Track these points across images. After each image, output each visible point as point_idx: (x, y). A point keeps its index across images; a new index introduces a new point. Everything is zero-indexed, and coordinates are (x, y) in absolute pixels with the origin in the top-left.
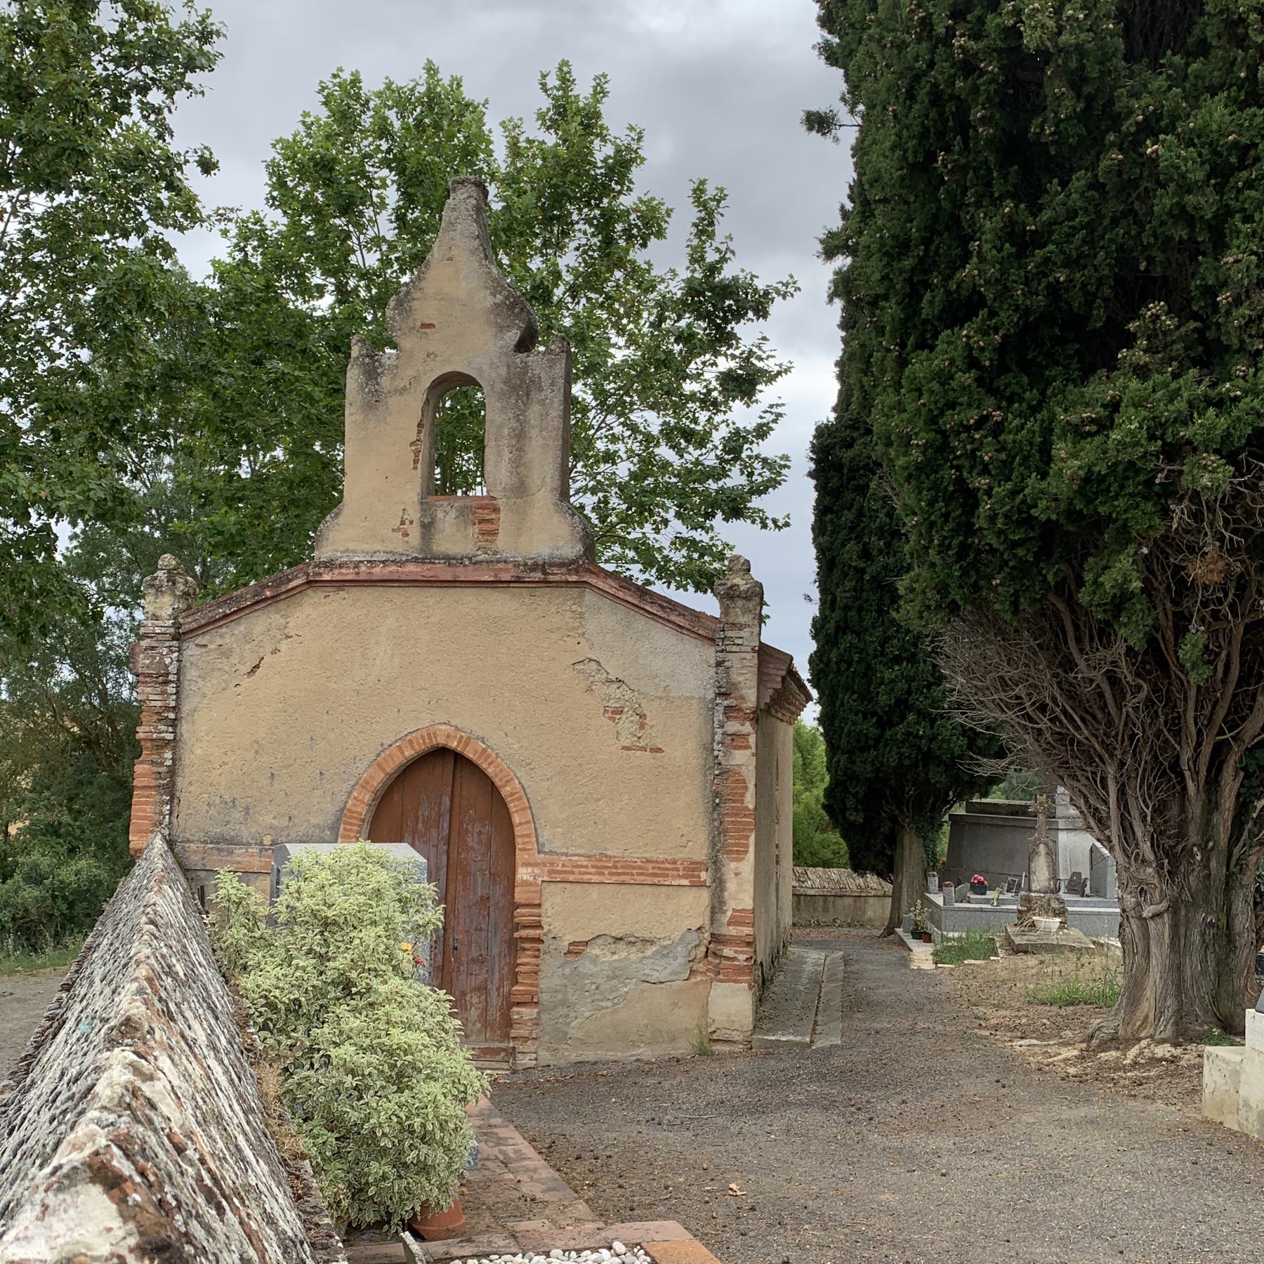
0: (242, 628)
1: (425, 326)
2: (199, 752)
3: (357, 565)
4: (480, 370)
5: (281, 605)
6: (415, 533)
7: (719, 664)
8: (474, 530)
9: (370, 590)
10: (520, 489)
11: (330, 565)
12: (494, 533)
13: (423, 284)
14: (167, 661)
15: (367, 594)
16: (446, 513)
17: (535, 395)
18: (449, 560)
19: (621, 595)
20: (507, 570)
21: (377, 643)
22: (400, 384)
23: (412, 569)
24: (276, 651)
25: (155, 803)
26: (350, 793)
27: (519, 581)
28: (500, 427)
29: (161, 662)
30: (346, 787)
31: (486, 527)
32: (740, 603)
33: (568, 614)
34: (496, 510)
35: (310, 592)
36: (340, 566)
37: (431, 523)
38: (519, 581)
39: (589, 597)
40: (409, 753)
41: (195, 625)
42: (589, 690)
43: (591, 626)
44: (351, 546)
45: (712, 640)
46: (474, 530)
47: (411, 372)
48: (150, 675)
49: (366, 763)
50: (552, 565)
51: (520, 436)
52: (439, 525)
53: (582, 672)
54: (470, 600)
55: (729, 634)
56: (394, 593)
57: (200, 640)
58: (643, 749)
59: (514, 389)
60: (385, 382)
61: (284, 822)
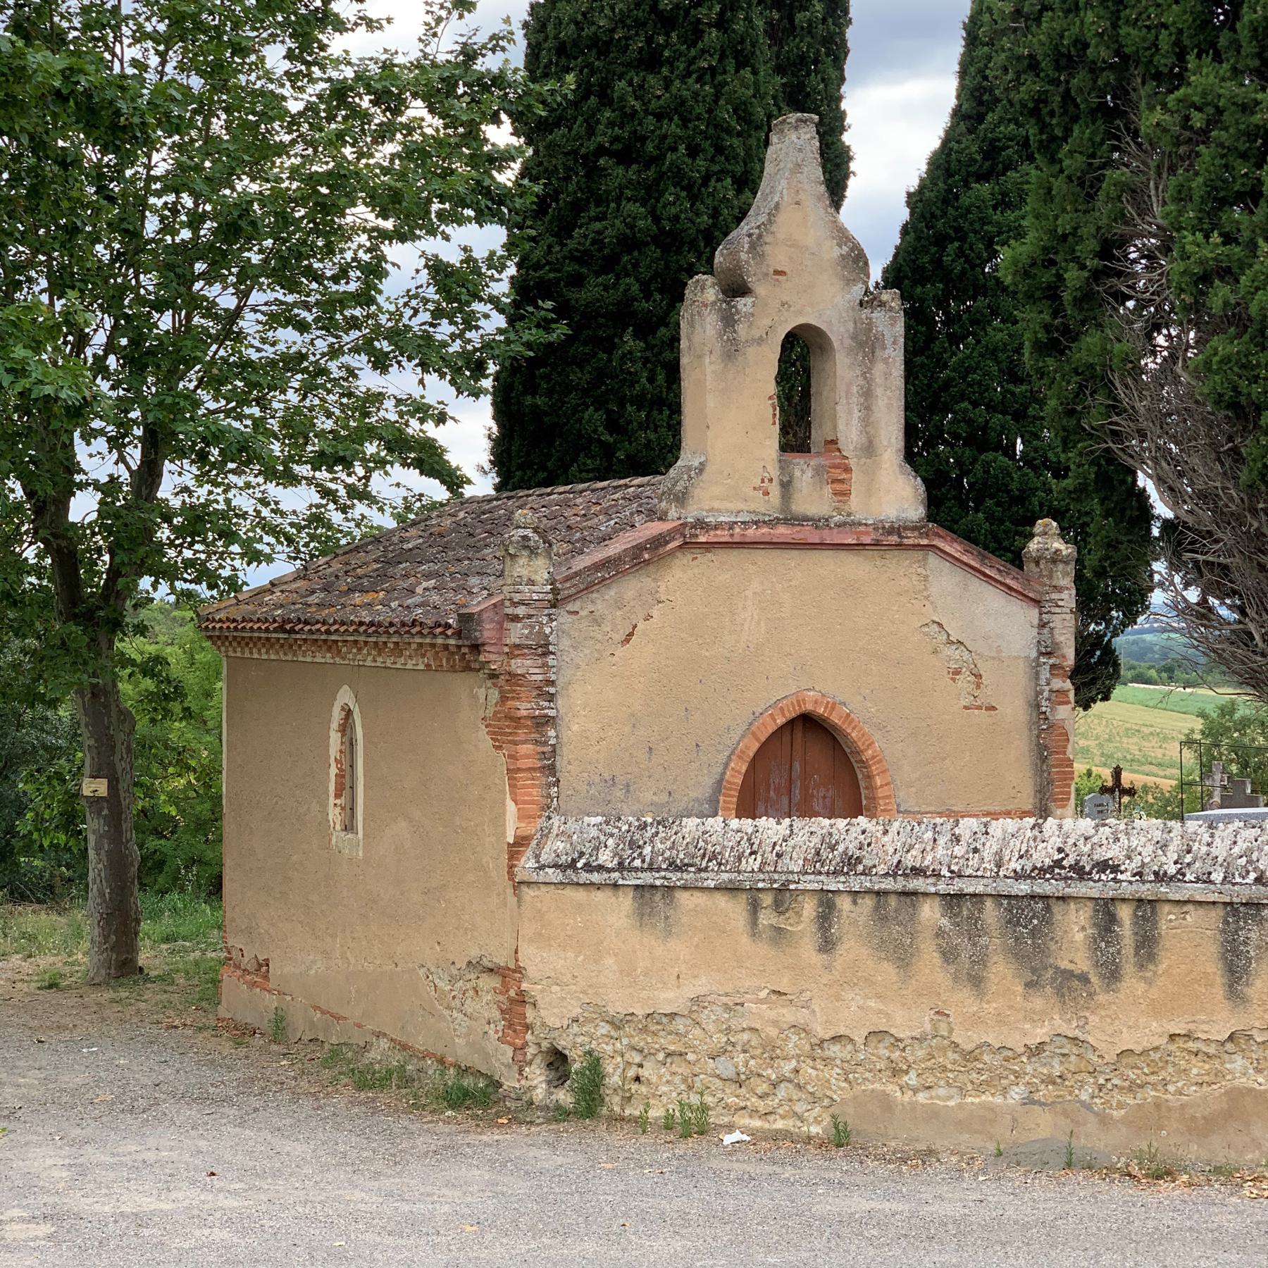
0: (612, 593)
1: (777, 272)
2: (575, 728)
3: (731, 525)
4: (830, 323)
5: (651, 568)
6: (775, 490)
7: (1042, 625)
8: (828, 489)
9: (735, 552)
10: (869, 449)
11: (701, 524)
12: (846, 494)
13: (773, 228)
14: (548, 630)
15: (734, 556)
16: (803, 471)
17: (878, 353)
18: (802, 520)
19: (965, 558)
20: (867, 533)
21: (744, 608)
22: (756, 333)
23: (782, 532)
24: (649, 617)
25: (540, 786)
26: (726, 765)
27: (877, 544)
28: (849, 385)
29: (541, 632)
30: (722, 758)
31: (838, 487)
32: (1061, 566)
33: (914, 577)
34: (847, 469)
35: (679, 554)
36: (716, 528)
37: (790, 482)
38: (877, 544)
39: (933, 560)
40: (781, 721)
41: (573, 590)
42: (935, 652)
43: (934, 590)
44: (716, 505)
45: (1037, 602)
46: (828, 489)
47: (767, 322)
48: (529, 647)
49: (740, 732)
50: (906, 528)
51: (867, 394)
52: (796, 484)
53: (926, 634)
54: (827, 563)
55: (1054, 596)
56: (760, 556)
57: (570, 607)
58: (979, 708)
59: (861, 345)
60: (741, 328)
61: (664, 798)
